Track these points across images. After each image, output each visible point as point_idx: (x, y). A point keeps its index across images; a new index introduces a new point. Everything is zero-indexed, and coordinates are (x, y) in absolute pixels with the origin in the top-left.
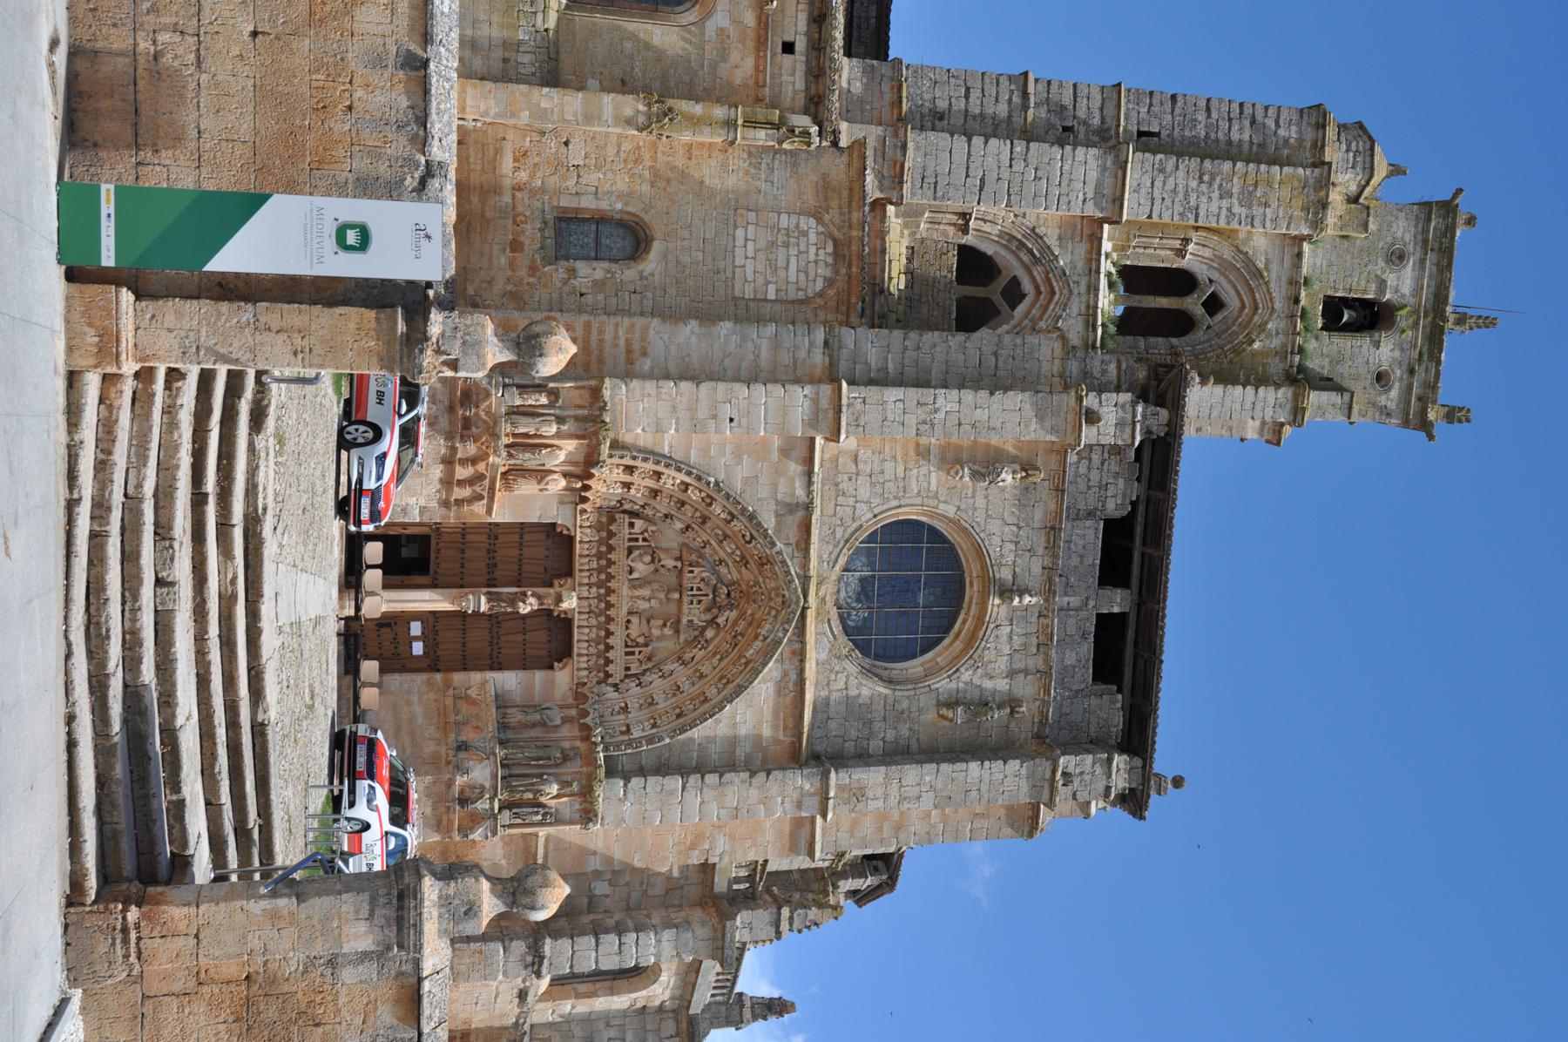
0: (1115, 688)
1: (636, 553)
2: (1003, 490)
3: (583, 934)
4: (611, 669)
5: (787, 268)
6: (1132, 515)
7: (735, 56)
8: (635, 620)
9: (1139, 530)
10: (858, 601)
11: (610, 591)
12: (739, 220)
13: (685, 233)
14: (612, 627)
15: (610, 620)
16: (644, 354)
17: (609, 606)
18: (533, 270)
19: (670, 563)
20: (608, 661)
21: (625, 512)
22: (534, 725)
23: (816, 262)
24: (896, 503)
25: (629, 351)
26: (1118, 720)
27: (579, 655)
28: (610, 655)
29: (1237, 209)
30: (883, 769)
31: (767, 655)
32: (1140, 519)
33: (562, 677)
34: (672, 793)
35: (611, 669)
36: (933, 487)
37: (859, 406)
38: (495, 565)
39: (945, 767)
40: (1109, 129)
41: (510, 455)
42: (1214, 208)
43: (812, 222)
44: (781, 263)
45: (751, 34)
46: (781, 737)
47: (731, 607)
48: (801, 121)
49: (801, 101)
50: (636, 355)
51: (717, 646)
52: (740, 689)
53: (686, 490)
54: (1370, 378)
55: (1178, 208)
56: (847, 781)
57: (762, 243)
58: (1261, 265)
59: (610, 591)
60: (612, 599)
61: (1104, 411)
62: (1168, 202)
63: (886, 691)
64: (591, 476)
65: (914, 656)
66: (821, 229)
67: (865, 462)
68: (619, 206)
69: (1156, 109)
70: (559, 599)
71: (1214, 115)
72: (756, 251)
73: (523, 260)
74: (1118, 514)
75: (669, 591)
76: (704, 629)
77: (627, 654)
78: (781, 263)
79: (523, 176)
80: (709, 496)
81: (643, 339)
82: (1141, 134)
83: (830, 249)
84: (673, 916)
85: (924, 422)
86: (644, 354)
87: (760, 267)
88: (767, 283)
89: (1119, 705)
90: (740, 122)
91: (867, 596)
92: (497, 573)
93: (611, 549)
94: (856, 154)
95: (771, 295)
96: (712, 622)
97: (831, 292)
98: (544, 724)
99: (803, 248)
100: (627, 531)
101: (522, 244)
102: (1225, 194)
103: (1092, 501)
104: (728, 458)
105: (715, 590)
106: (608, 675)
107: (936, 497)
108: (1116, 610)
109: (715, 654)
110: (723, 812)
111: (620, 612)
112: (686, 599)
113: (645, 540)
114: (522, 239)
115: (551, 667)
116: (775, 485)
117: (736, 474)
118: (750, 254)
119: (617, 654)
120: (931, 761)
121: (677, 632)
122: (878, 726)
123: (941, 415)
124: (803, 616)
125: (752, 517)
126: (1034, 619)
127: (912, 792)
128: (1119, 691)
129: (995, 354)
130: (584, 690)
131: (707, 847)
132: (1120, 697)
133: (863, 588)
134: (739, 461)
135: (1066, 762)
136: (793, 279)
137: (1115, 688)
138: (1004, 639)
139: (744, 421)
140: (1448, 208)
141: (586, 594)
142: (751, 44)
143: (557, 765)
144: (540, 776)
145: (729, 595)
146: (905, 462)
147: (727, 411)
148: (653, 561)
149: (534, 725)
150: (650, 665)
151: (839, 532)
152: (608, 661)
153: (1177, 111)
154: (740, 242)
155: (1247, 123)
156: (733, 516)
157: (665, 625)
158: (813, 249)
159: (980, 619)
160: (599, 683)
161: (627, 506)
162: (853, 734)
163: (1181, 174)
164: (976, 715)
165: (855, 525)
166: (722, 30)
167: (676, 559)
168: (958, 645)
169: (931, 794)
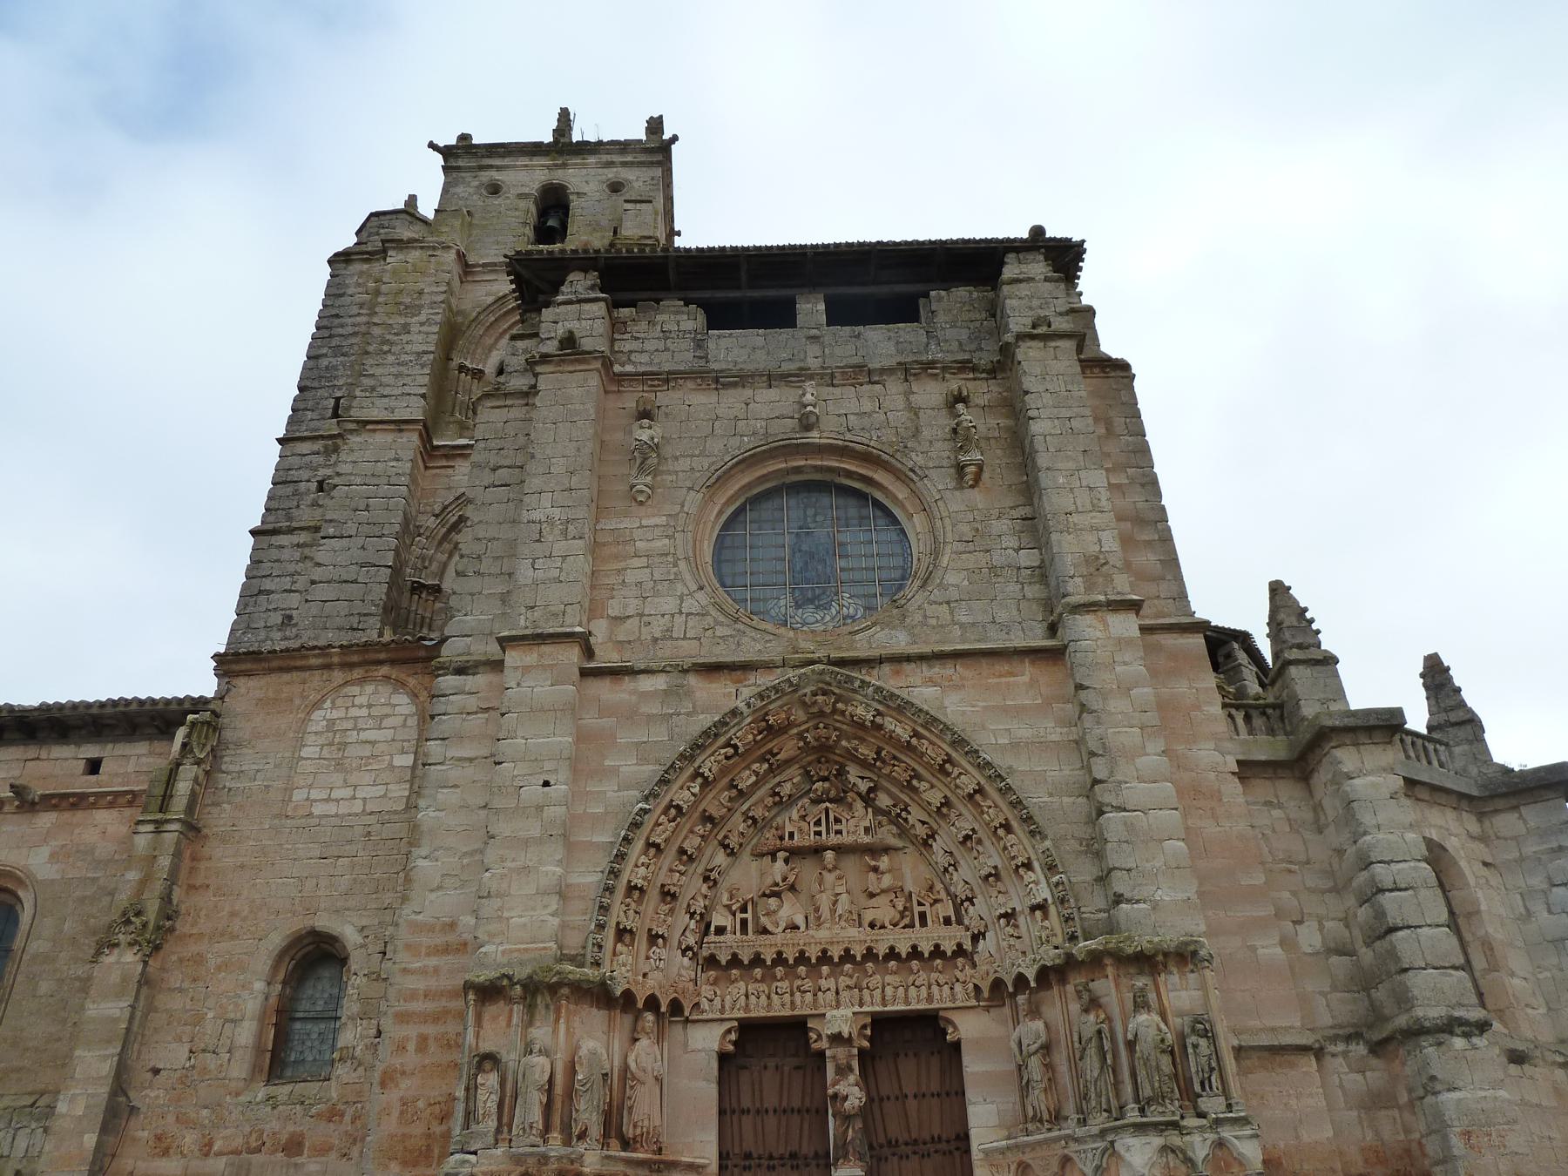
0: (922, 301)
1: (764, 920)
3: (1393, 954)
4: (949, 947)
5: (373, 743)
6: (701, 304)
7: (90, 836)
8: (868, 916)
9: (720, 295)
10: (827, 607)
11: (824, 958)
12: (301, 812)
13: (310, 884)
14: (882, 950)
15: (870, 955)
16: (452, 926)
17: (847, 956)
18: (333, 1115)
19: (780, 864)
20: (937, 952)
21: (700, 943)
22: (1049, 1067)
23: (370, 706)
24: (682, 565)
25: (446, 950)
26: (962, 292)
27: (930, 998)
28: (926, 948)
29: (423, 318)
30: (1054, 537)
31: (903, 708)
32: (707, 294)
33: (969, 1027)
34: (1129, 827)
35: (949, 947)
36: (662, 520)
37: (537, 614)
38: (793, 1156)
39: (1042, 460)
40: (326, 447)
41: (582, 1136)
42: (420, 338)
43: (317, 715)
44: (366, 751)
45: (67, 815)
46: (1026, 678)
47: (841, 773)
48: (181, 734)
49: (159, 746)
50: (451, 938)
51: (902, 788)
52: (959, 742)
53: (657, 846)
54: (614, 197)
55: (417, 370)
56: (1078, 580)
57: (337, 778)
58: (491, 299)
59: (824, 958)
60: (836, 953)
61: (561, 331)
62: (408, 380)
63: (948, 550)
64: (628, 996)
65: (903, 531)
66: (328, 704)
67: (626, 606)
68: (259, 986)
69: (310, 404)
70: (837, 1039)
71: (324, 351)
72: (346, 785)
73: (317, 1132)
74: (701, 317)
75: (825, 868)
76: (878, 811)
77: (923, 923)
78: (366, 751)
79: (190, 1139)
80: (665, 812)
81: (431, 929)
82: (335, 415)
83: (355, 690)
84: (1331, 815)
85: (565, 533)
86: (452, 926)
87: (367, 778)
88: (391, 767)
89: (943, 293)
90: (159, 816)
91: (818, 597)
92: (805, 1150)
93: (757, 960)
94: (235, 667)
95: (408, 760)
96: (868, 799)
97: (412, 681)
98: (1047, 1048)
99: (350, 725)
100: (727, 937)
101: (293, 1135)
102: (406, 329)
103: (687, 344)
104: (609, 789)
105: (816, 802)
106: (960, 951)
108: (822, 307)
109: (915, 790)
110: (1150, 748)
111: (856, 938)
112: (834, 839)
113: (744, 909)
114: (284, 1138)
115: (957, 1046)
116: (650, 717)
117: (627, 773)
118: (348, 792)
119: (925, 939)
120: (1037, 480)
121: (887, 850)
122: (998, 558)
123: (557, 513)
124: (842, 663)
125: (697, 747)
126: (837, 391)
127: (1084, 499)
128: (927, 296)
129: (494, 470)
130: (986, 988)
131: (1212, 775)
132: (933, 293)
133: (811, 601)
134: (615, 771)
135: (1018, 322)
136: (389, 734)
137: (922, 301)
138: (866, 421)
139: (548, 766)
140: (446, 152)
141: (830, 996)
142: (79, 815)
143: (1109, 1019)
144: (1131, 1045)
145: (825, 779)
146: (625, 558)
147: (532, 792)
148: (777, 895)
149: (1049, 1067)
150: (939, 886)
151: (720, 631)
152: (937, 952)
153: (316, 384)
154: (331, 809)
155: (337, 321)
156: (697, 774)
157: (875, 869)
158: (354, 712)
159: (843, 451)
160: (974, 966)
161: (691, 940)
162: (1013, 588)
163: (378, 371)
164: (967, 439)
165: (714, 613)
166: (52, 855)
167: (774, 859)
168: (879, 476)
169: (1083, 474)
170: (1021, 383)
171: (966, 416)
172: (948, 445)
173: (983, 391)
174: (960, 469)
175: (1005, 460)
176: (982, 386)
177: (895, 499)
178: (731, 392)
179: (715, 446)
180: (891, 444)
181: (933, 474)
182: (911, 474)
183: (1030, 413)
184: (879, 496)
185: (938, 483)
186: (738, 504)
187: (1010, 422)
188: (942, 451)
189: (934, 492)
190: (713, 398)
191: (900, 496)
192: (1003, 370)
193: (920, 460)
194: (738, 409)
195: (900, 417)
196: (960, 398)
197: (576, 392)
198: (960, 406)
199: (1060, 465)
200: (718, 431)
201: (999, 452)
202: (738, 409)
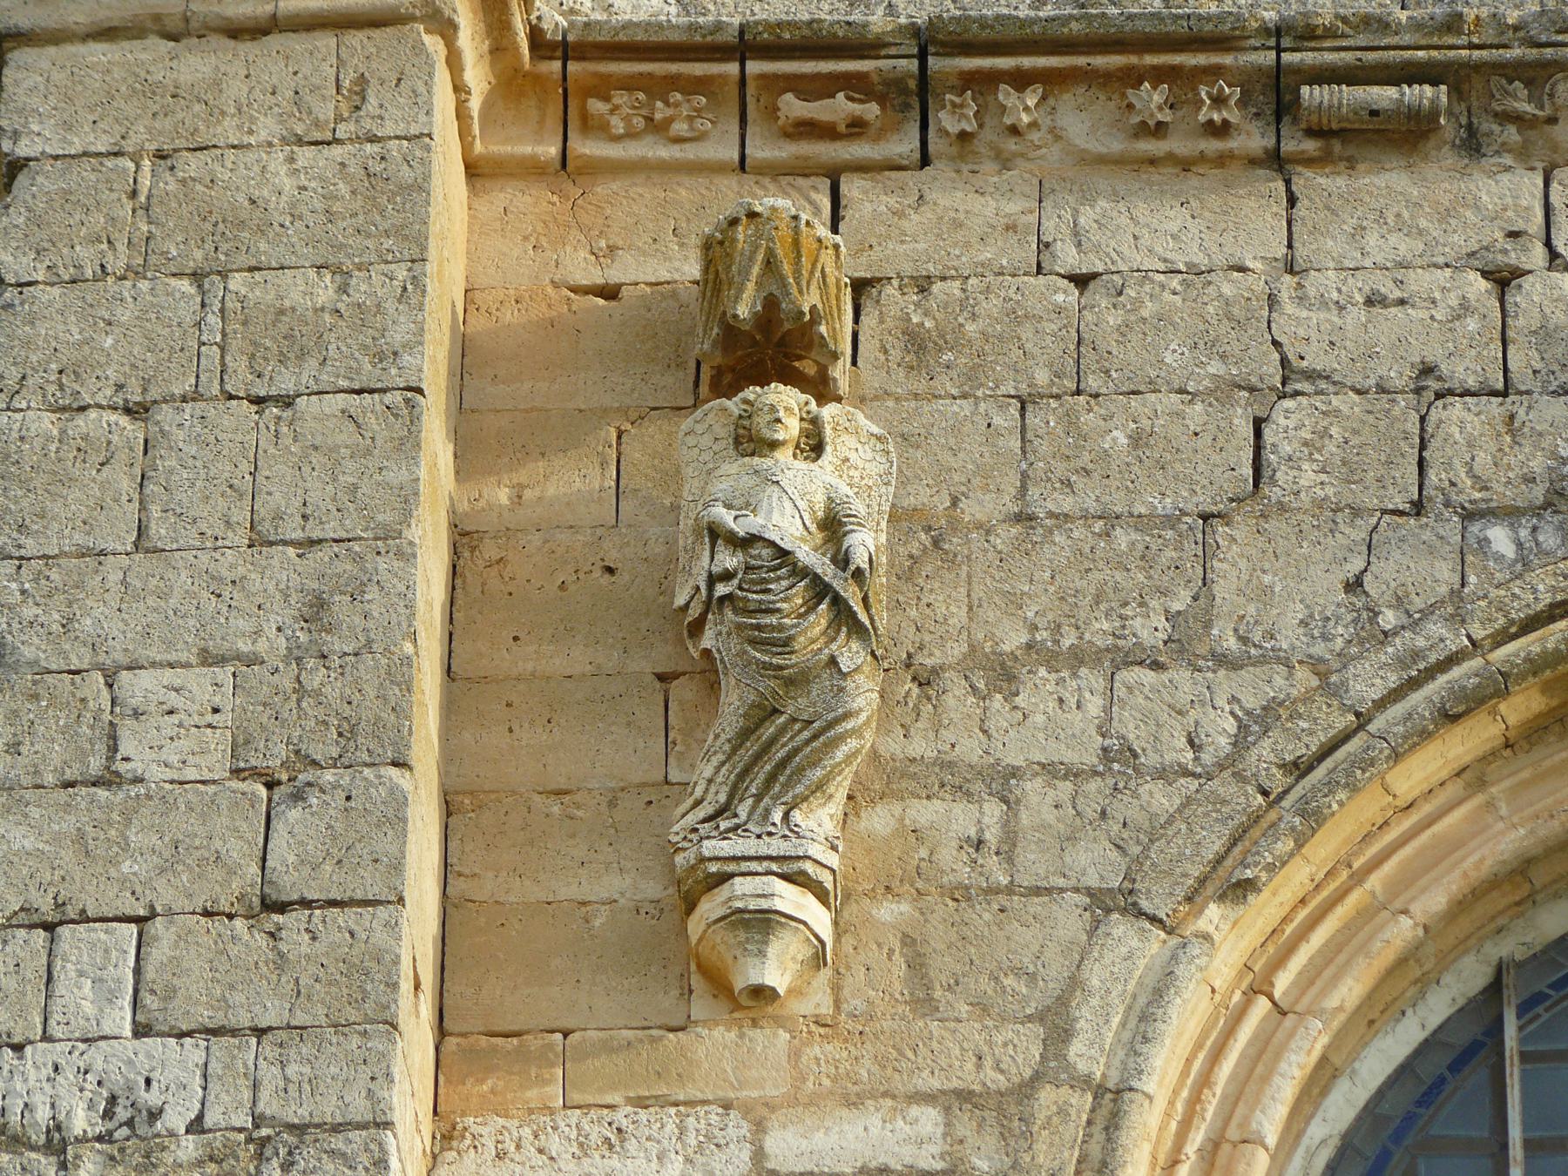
2: (928, 535)
107: (1006, 1108)
178: (1388, 183)
179: (1282, 586)
186: (1438, 1008)
190: (1252, 223)
194: (1444, 316)
197: (282, 178)
200: (1299, 479)
202: (1444, 316)
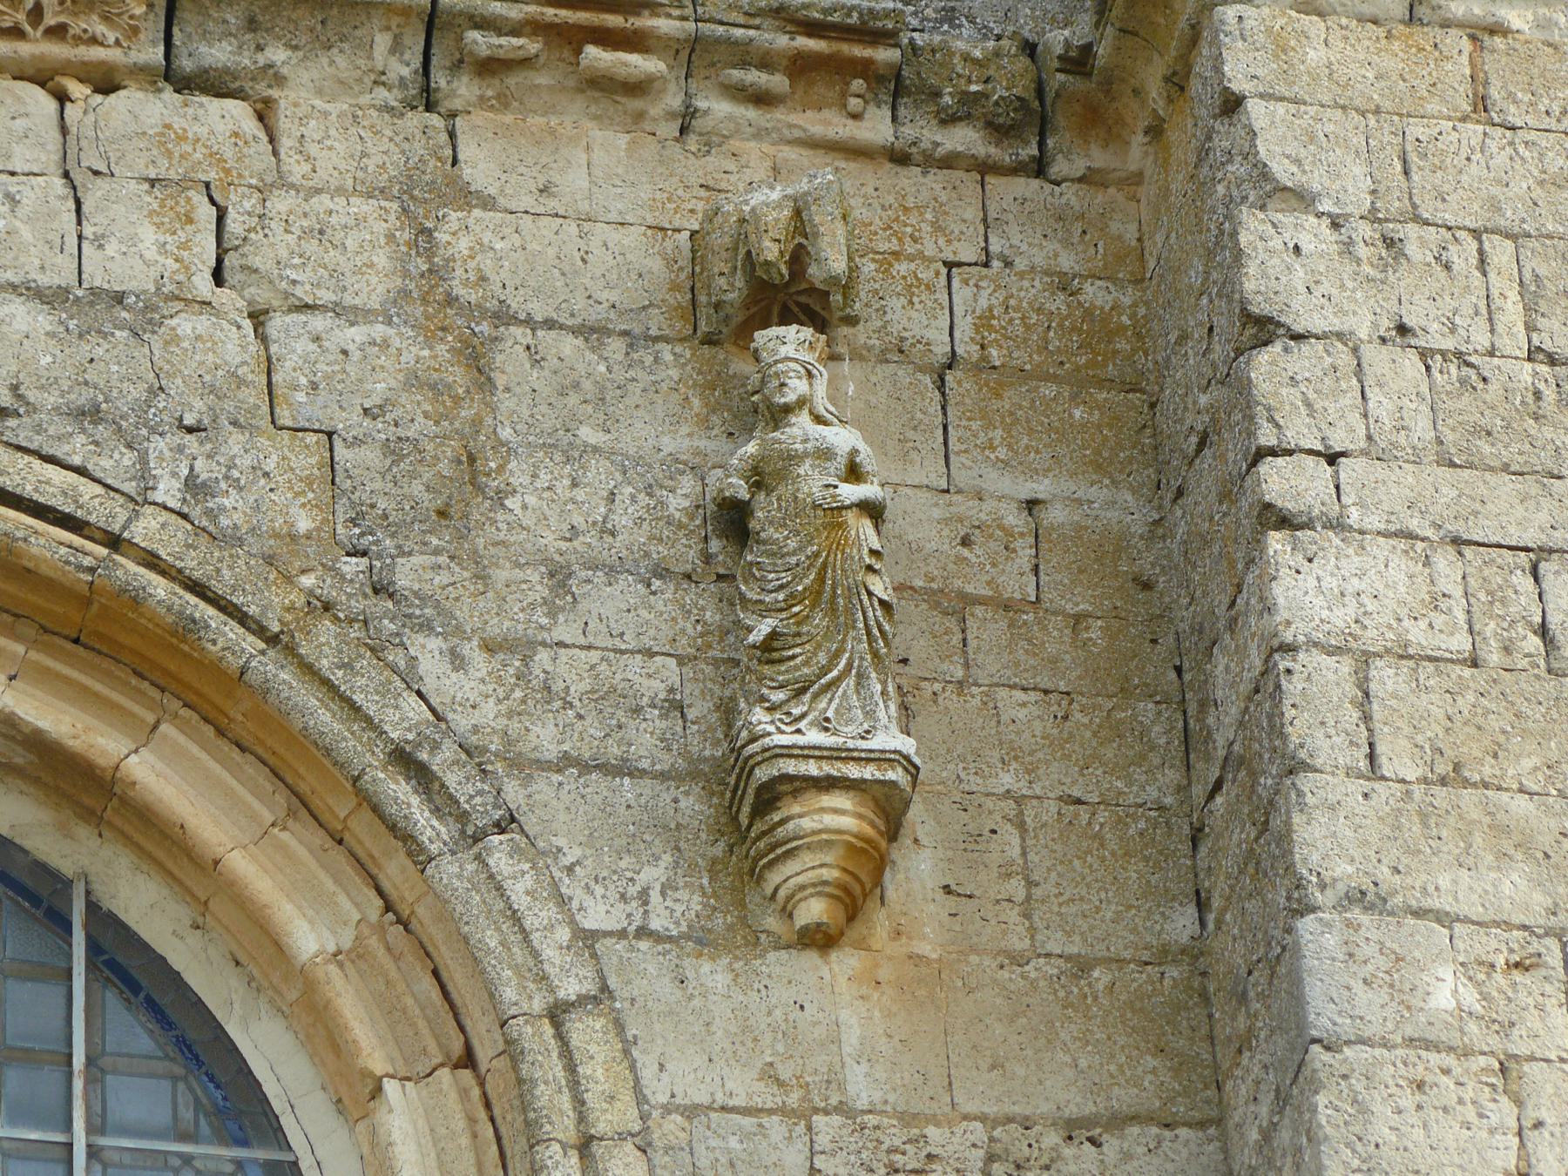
39: (1334, 831)
120: (1279, 963)
138: (116, 364)
164: (825, 593)
168: (166, 771)
170: (1225, 253)
171: (830, 415)
172: (662, 614)
173: (935, 248)
174: (747, 805)
175: (1056, 777)
176: (942, 216)
177: (260, 950)
180: (279, 559)
181: (552, 805)
182: (400, 792)
183: (1279, 482)
184: (144, 905)
185: (577, 887)
187: (1119, 507)
188: (630, 638)
189: (553, 946)
191: (308, 939)
192: (1098, 120)
193: (472, 693)
195: (351, 362)
196: (790, 292)
198: (788, 343)
199: (1452, 887)
201: (1019, 708)
